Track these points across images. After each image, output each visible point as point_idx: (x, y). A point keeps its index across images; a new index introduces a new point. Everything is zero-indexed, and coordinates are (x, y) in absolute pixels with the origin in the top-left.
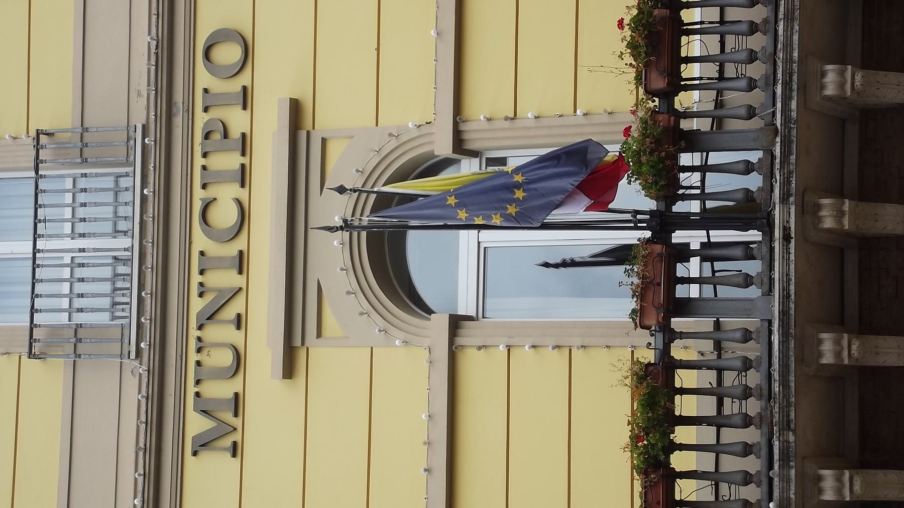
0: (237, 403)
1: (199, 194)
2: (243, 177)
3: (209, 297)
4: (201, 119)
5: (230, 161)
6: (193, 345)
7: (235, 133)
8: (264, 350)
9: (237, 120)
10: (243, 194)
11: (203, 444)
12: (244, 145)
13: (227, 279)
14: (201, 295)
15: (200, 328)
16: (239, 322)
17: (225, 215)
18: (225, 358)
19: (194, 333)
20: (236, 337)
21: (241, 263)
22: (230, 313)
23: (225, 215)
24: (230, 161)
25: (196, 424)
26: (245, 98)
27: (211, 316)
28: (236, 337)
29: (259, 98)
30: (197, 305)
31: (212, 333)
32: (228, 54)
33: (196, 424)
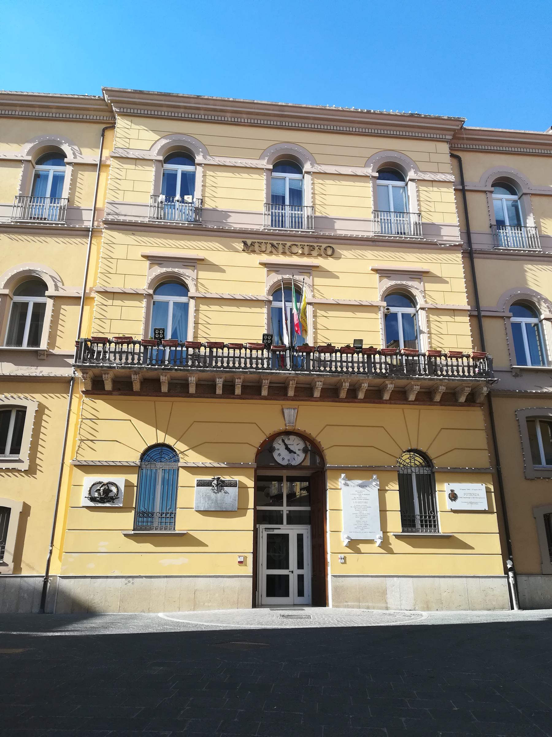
0: (254, 252)
1: (299, 244)
2: (303, 254)
3: (277, 246)
4: (315, 245)
5: (306, 252)
6: (266, 241)
7: (312, 252)
9: (315, 253)
11: (245, 243)
12: (310, 255)
19: (269, 242)
23: (295, 249)
27: (273, 245)
30: (275, 243)
31: (269, 246)
32: (329, 252)
33: (249, 242)
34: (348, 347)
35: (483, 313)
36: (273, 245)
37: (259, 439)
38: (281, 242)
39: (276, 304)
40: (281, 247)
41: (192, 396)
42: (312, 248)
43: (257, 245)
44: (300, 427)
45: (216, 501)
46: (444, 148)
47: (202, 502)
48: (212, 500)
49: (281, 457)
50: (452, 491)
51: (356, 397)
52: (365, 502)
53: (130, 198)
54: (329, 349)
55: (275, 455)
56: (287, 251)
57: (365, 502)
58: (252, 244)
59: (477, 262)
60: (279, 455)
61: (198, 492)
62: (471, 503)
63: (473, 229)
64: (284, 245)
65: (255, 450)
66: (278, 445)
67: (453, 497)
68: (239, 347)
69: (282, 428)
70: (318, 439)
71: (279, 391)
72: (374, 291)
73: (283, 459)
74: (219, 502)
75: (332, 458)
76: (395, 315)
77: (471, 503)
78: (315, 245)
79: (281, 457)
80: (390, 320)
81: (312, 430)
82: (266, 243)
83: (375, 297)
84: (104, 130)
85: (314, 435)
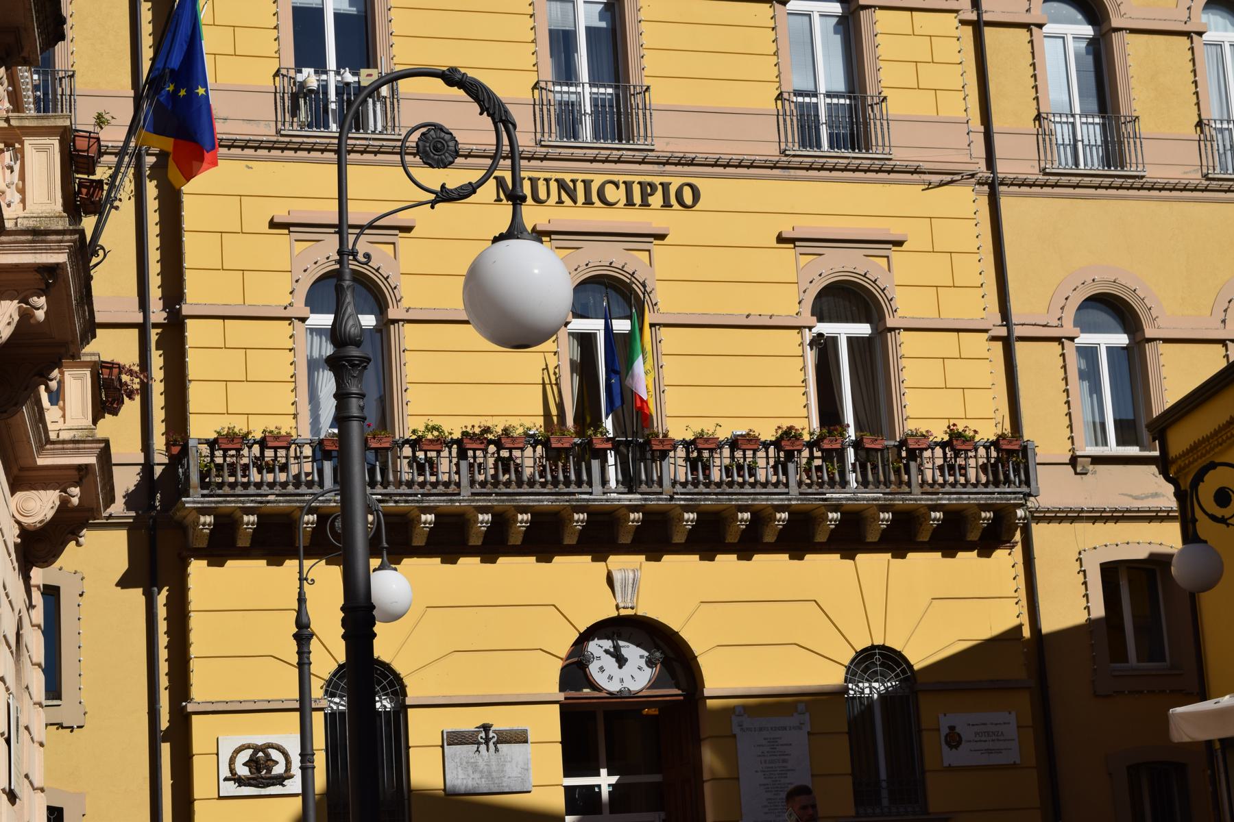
1: (621, 179)
2: (630, 203)
3: (571, 185)
5: (637, 199)
6: (548, 175)
9: (656, 200)
10: (621, 204)
12: (645, 204)
14: (572, 181)
15: (556, 180)
16: (560, 202)
17: (611, 193)
21: (588, 202)
22: (564, 197)
24: (637, 199)
27: (561, 184)
29: (667, 213)
30: (567, 178)
31: (554, 186)
32: (688, 196)
35: (1018, 331)
36: (561, 184)
38: (581, 177)
42: (648, 190)
44: (647, 608)
45: (490, 773)
47: (461, 776)
48: (481, 772)
49: (606, 674)
50: (952, 728)
52: (784, 761)
55: (593, 669)
56: (595, 198)
57: (784, 761)
59: (1005, 203)
60: (602, 669)
62: (989, 751)
63: (997, 124)
65: (559, 665)
66: (596, 647)
67: (954, 740)
71: (601, 537)
72: (787, 288)
73: (610, 678)
74: (494, 775)
76: (834, 340)
77: (989, 751)
78: (657, 180)
79: (606, 674)
82: (547, 180)
83: (792, 302)
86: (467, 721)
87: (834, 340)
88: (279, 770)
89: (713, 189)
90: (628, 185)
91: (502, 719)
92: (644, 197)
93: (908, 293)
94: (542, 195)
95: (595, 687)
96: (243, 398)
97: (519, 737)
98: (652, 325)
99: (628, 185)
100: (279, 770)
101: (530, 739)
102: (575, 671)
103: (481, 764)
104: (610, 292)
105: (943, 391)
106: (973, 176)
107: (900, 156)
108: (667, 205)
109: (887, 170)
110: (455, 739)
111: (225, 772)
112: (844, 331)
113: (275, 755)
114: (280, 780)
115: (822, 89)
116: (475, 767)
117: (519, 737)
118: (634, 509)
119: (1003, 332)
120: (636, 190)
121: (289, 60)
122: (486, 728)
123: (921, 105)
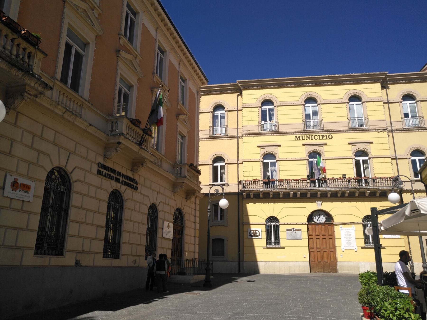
0: (300, 140)
2: (320, 139)
5: (321, 138)
8: (305, 142)
11: (296, 137)
12: (322, 139)
13: (311, 138)
17: (316, 137)
18: (304, 139)
20: (306, 139)
21: (312, 139)
22: (308, 139)
23: (316, 137)
24: (321, 138)
25: (298, 136)
26: (326, 139)
27: (307, 136)
28: (306, 139)
30: (308, 135)
31: (306, 137)
33: (298, 136)
34: (340, 178)
35: (398, 157)
36: (307, 136)
37: (308, 214)
39: (310, 160)
40: (310, 137)
41: (281, 198)
42: (323, 136)
43: (301, 137)
46: (379, 85)
51: (344, 196)
53: (251, 123)
54: (333, 179)
58: (299, 137)
61: (287, 233)
64: (312, 136)
68: (298, 180)
69: (316, 209)
70: (330, 213)
72: (350, 151)
75: (336, 220)
76: (359, 161)
78: (324, 135)
80: (357, 163)
81: (328, 210)
83: (351, 154)
84: (238, 96)
85: (328, 211)
86: (290, 227)
87: (359, 161)
88: (258, 234)
89: (335, 135)
90: (319, 136)
91: (296, 227)
92: (322, 137)
93: (373, 151)
94: (304, 139)
95: (315, 222)
96: (252, 174)
97: (300, 230)
98: (323, 159)
99: (319, 136)
100: (258, 234)
101: (302, 230)
102: (310, 218)
103: (293, 235)
104: (314, 154)
105: (380, 169)
106: (386, 129)
107: (371, 127)
108: (326, 139)
109: (369, 130)
110: (288, 230)
111: (249, 234)
112: (361, 159)
113: (257, 232)
114: (258, 236)
115: (356, 116)
116: (291, 235)
117: (300, 230)
118: (319, 191)
119: (395, 157)
120: (321, 137)
121: (261, 121)
122: (294, 228)
123: (377, 118)
